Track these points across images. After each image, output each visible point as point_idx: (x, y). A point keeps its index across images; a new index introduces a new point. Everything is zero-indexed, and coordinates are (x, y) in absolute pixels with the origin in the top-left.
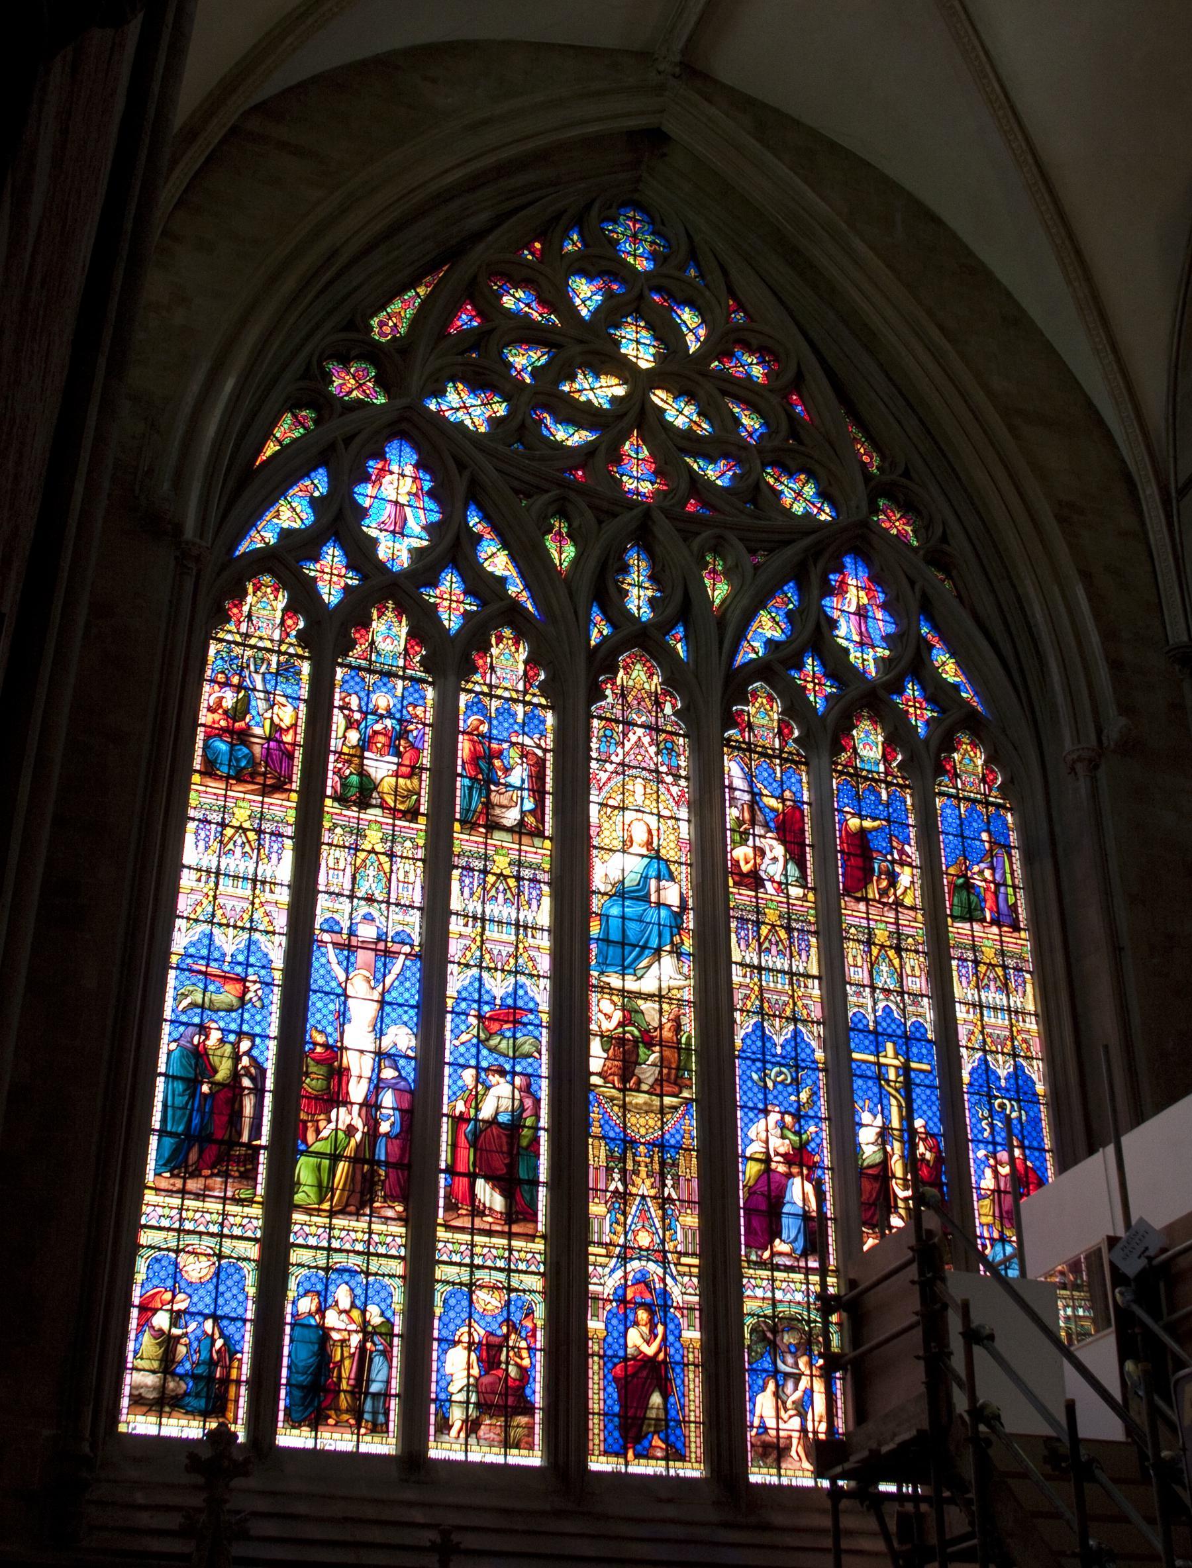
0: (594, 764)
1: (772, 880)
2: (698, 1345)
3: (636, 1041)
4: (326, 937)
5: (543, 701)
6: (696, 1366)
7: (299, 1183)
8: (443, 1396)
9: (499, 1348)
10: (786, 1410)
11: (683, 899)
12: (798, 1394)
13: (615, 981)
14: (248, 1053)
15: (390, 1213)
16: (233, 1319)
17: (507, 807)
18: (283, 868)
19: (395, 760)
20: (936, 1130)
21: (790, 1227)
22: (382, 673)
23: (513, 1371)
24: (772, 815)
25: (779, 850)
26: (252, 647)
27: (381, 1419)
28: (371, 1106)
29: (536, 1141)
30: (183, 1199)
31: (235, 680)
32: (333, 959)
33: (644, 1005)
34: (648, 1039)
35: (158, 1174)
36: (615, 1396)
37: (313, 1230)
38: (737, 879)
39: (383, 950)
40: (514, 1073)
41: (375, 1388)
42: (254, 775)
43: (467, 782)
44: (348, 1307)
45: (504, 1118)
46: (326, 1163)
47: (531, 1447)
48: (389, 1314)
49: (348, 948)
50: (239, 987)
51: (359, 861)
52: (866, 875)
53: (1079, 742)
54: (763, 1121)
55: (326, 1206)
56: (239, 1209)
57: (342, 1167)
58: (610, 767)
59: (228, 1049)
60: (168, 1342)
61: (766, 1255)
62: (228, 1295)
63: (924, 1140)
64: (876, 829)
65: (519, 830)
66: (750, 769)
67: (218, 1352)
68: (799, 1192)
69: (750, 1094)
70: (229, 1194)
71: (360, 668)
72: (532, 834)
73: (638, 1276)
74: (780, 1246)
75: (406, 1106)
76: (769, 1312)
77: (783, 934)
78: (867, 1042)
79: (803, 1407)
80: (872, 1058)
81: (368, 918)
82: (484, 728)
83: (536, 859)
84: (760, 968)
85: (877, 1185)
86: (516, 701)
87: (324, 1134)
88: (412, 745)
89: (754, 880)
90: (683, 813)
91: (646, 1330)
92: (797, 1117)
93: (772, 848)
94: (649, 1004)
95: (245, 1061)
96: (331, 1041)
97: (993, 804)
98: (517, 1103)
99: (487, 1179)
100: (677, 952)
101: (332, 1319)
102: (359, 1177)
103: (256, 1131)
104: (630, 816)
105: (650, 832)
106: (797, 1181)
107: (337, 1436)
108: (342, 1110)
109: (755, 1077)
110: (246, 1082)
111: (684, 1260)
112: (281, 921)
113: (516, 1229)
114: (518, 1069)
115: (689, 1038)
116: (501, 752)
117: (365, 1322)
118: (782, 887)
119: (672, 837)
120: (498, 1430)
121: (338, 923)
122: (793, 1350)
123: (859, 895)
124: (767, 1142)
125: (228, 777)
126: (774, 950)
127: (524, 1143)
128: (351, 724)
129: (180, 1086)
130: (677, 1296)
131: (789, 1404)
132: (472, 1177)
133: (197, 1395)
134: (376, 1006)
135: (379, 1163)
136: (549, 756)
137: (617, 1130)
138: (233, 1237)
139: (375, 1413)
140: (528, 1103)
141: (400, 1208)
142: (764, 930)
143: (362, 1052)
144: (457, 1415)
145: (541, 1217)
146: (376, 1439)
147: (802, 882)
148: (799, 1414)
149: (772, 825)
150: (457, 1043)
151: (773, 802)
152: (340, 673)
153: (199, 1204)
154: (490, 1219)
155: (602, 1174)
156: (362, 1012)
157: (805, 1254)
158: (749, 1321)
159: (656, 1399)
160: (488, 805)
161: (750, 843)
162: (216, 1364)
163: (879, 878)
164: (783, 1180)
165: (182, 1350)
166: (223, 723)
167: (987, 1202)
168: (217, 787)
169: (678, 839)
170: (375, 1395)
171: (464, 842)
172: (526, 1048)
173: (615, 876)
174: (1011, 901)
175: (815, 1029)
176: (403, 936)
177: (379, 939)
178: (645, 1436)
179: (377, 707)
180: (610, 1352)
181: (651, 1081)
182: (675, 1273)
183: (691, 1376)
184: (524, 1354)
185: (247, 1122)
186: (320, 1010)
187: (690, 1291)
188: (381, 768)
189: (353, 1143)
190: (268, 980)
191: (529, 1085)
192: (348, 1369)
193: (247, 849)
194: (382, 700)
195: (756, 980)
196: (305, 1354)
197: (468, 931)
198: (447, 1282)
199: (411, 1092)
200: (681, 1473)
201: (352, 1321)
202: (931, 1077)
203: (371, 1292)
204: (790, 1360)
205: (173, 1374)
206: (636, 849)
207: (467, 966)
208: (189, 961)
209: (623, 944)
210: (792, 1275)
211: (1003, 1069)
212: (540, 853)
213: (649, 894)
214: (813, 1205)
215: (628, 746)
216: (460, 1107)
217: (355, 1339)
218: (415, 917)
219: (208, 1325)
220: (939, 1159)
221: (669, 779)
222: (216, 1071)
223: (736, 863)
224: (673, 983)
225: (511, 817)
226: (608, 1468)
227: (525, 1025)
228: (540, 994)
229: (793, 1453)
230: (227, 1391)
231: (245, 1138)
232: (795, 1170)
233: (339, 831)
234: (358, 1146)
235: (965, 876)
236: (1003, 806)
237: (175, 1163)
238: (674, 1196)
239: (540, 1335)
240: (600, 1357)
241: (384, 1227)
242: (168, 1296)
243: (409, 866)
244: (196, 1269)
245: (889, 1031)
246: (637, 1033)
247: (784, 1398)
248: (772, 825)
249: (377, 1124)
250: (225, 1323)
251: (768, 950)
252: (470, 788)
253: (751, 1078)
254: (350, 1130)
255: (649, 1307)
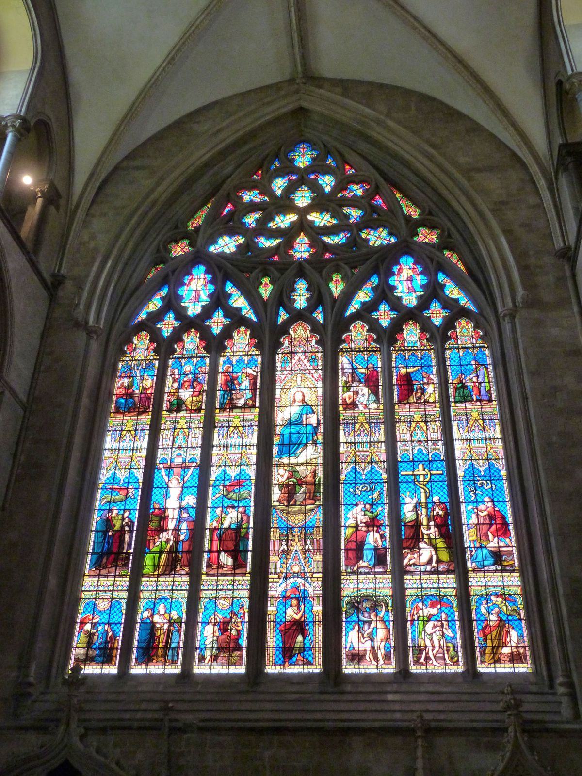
0: (278, 373)
1: (362, 404)
2: (321, 612)
3: (295, 484)
4: (161, 466)
5: (257, 353)
6: (320, 622)
7: (146, 565)
8: (202, 647)
9: (228, 623)
10: (364, 638)
11: (318, 420)
12: (370, 630)
13: (286, 461)
14: (127, 517)
15: (183, 572)
16: (116, 624)
17: (239, 399)
18: (144, 442)
19: (192, 390)
20: (445, 501)
21: (368, 555)
22: (188, 358)
23: (234, 633)
24: (363, 376)
25: (366, 390)
26: (136, 360)
27: (175, 658)
28: (177, 530)
29: (247, 533)
30: (99, 578)
31: (129, 375)
32: (164, 474)
33: (298, 468)
34: (300, 483)
35: (90, 570)
36: (281, 639)
37: (151, 583)
38: (345, 406)
39: (184, 467)
40: (238, 507)
41: (173, 646)
42: (134, 409)
43: (222, 392)
44: (163, 613)
45: (233, 526)
46: (157, 555)
47: (241, 665)
48: (180, 614)
49: (170, 468)
50: (126, 491)
51: (176, 433)
52: (410, 391)
53: (504, 307)
54: (355, 510)
55: (156, 573)
56: (121, 579)
57: (164, 556)
58: (285, 372)
59: (120, 516)
60: (90, 636)
61: (355, 568)
62: (115, 614)
63: (438, 506)
64: (415, 371)
65: (245, 407)
66: (352, 358)
67: (110, 637)
68: (372, 538)
69: (349, 498)
70: (117, 574)
71: (179, 358)
72: (250, 407)
73: (293, 585)
74: (362, 563)
75: (192, 527)
76: (356, 594)
77: (367, 426)
78: (409, 466)
79: (371, 637)
80: (411, 473)
81: (179, 455)
82: (230, 370)
83: (251, 417)
84: (355, 443)
85: (413, 530)
86: (244, 355)
87: (157, 544)
88: (200, 383)
89: (353, 405)
90: (320, 384)
91: (296, 608)
92: (372, 505)
93: (362, 390)
94: (301, 467)
95: (127, 520)
96: (161, 507)
97: (477, 347)
98: (239, 519)
99: (225, 552)
100: (315, 443)
101: (156, 619)
102: (170, 558)
103: (129, 547)
104: (293, 391)
105: (303, 395)
106: (372, 533)
107: (156, 667)
108: (165, 533)
109: (352, 490)
110: (127, 528)
111: (315, 575)
112: (143, 463)
113: (237, 571)
114: (241, 505)
115: (320, 479)
116: (238, 377)
117: (170, 618)
118: (366, 406)
119: (314, 395)
120: (226, 658)
121: (166, 459)
122: (368, 610)
123: (406, 402)
124: (356, 518)
125: (125, 412)
126: (362, 434)
127: (242, 535)
128: (174, 380)
129: (100, 534)
130: (311, 591)
131: (365, 635)
132: (219, 552)
133: (101, 656)
134: (180, 489)
135: (179, 552)
136: (259, 374)
137: (285, 523)
138: (118, 590)
139: (173, 656)
140: (245, 518)
141: (187, 570)
142: (357, 426)
143: (174, 509)
144: (208, 654)
145: (249, 565)
146: (173, 667)
147: (377, 401)
148: (371, 639)
149: (363, 380)
150: (214, 498)
151: (363, 371)
152: (170, 362)
153: (106, 579)
154: (226, 569)
155: (278, 543)
156: (174, 492)
157: (374, 566)
158: (346, 600)
159: (300, 638)
160: (231, 399)
161: (351, 390)
162: (109, 642)
163: (416, 392)
164: (365, 533)
165: (96, 638)
166: (124, 392)
167: (473, 530)
168: (119, 417)
169: (317, 396)
170: (173, 649)
171: (220, 416)
172: (245, 495)
173: (287, 416)
174: (488, 388)
175: (382, 465)
176: (193, 459)
177: (183, 463)
178: (294, 656)
179: (185, 371)
180: (278, 620)
181: (301, 500)
182: (310, 581)
183: (317, 626)
184: (239, 624)
185: (126, 544)
186: (157, 496)
187: (318, 589)
188: (186, 395)
189: (169, 546)
190: (137, 487)
191: (245, 511)
192: (163, 639)
193: (131, 438)
194: (188, 368)
195: (353, 448)
196: (145, 635)
197: (221, 452)
198: (206, 598)
199: (194, 521)
200: (311, 671)
201: (165, 618)
202: (443, 477)
203: (173, 606)
204: (366, 615)
205: (91, 648)
206: (297, 404)
207: (220, 466)
208: (106, 485)
209: (289, 445)
210: (368, 576)
211: (482, 466)
212: (253, 415)
213: (302, 421)
214: (380, 543)
215: (294, 361)
216: (215, 524)
217: (166, 626)
218: (198, 451)
219: (106, 627)
220: (446, 514)
221: (313, 371)
222: (115, 526)
223: (344, 400)
224: (313, 457)
225: (241, 402)
226: (276, 671)
227: (244, 486)
228: (251, 472)
229: (367, 657)
230: (113, 653)
231: (125, 551)
232: (370, 529)
233: (168, 423)
234: (171, 547)
235: (461, 382)
236: (484, 347)
237: (98, 565)
238: (311, 548)
239: (247, 616)
240: (274, 622)
241: (180, 578)
242: (91, 617)
243: (197, 431)
244: (103, 605)
245: (421, 459)
246: (295, 481)
247: (363, 632)
248: (363, 380)
249: (179, 536)
250: (113, 625)
251: (359, 434)
252: (224, 395)
253: (349, 491)
254: (168, 541)
255: (297, 598)
